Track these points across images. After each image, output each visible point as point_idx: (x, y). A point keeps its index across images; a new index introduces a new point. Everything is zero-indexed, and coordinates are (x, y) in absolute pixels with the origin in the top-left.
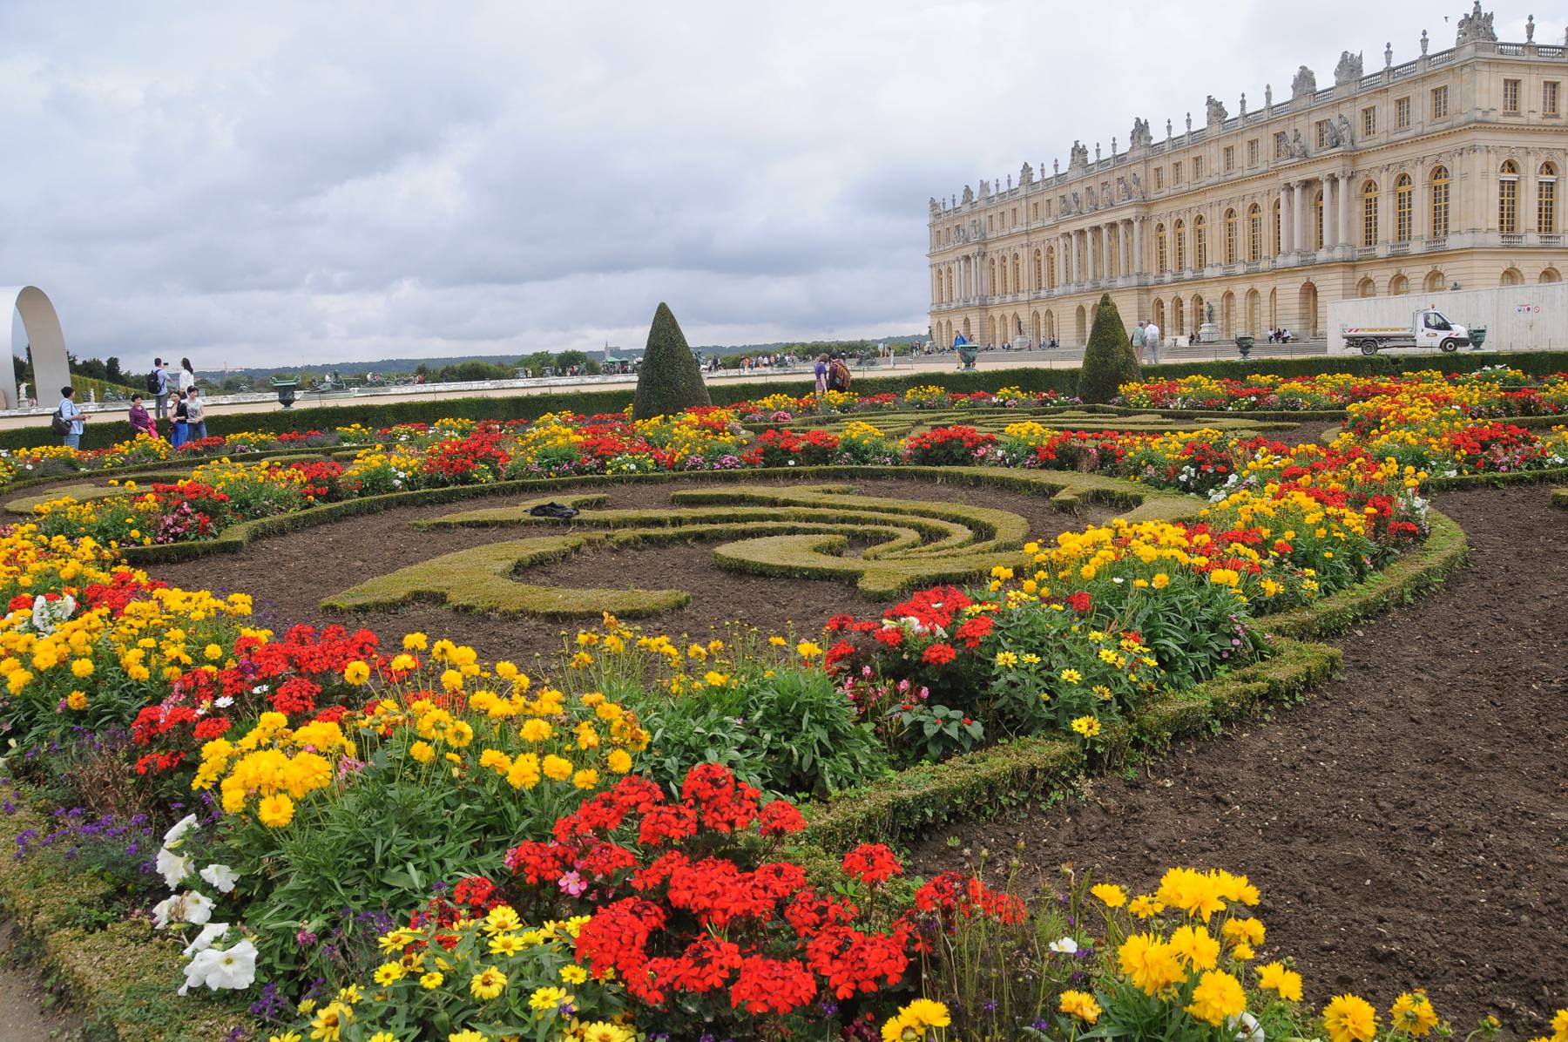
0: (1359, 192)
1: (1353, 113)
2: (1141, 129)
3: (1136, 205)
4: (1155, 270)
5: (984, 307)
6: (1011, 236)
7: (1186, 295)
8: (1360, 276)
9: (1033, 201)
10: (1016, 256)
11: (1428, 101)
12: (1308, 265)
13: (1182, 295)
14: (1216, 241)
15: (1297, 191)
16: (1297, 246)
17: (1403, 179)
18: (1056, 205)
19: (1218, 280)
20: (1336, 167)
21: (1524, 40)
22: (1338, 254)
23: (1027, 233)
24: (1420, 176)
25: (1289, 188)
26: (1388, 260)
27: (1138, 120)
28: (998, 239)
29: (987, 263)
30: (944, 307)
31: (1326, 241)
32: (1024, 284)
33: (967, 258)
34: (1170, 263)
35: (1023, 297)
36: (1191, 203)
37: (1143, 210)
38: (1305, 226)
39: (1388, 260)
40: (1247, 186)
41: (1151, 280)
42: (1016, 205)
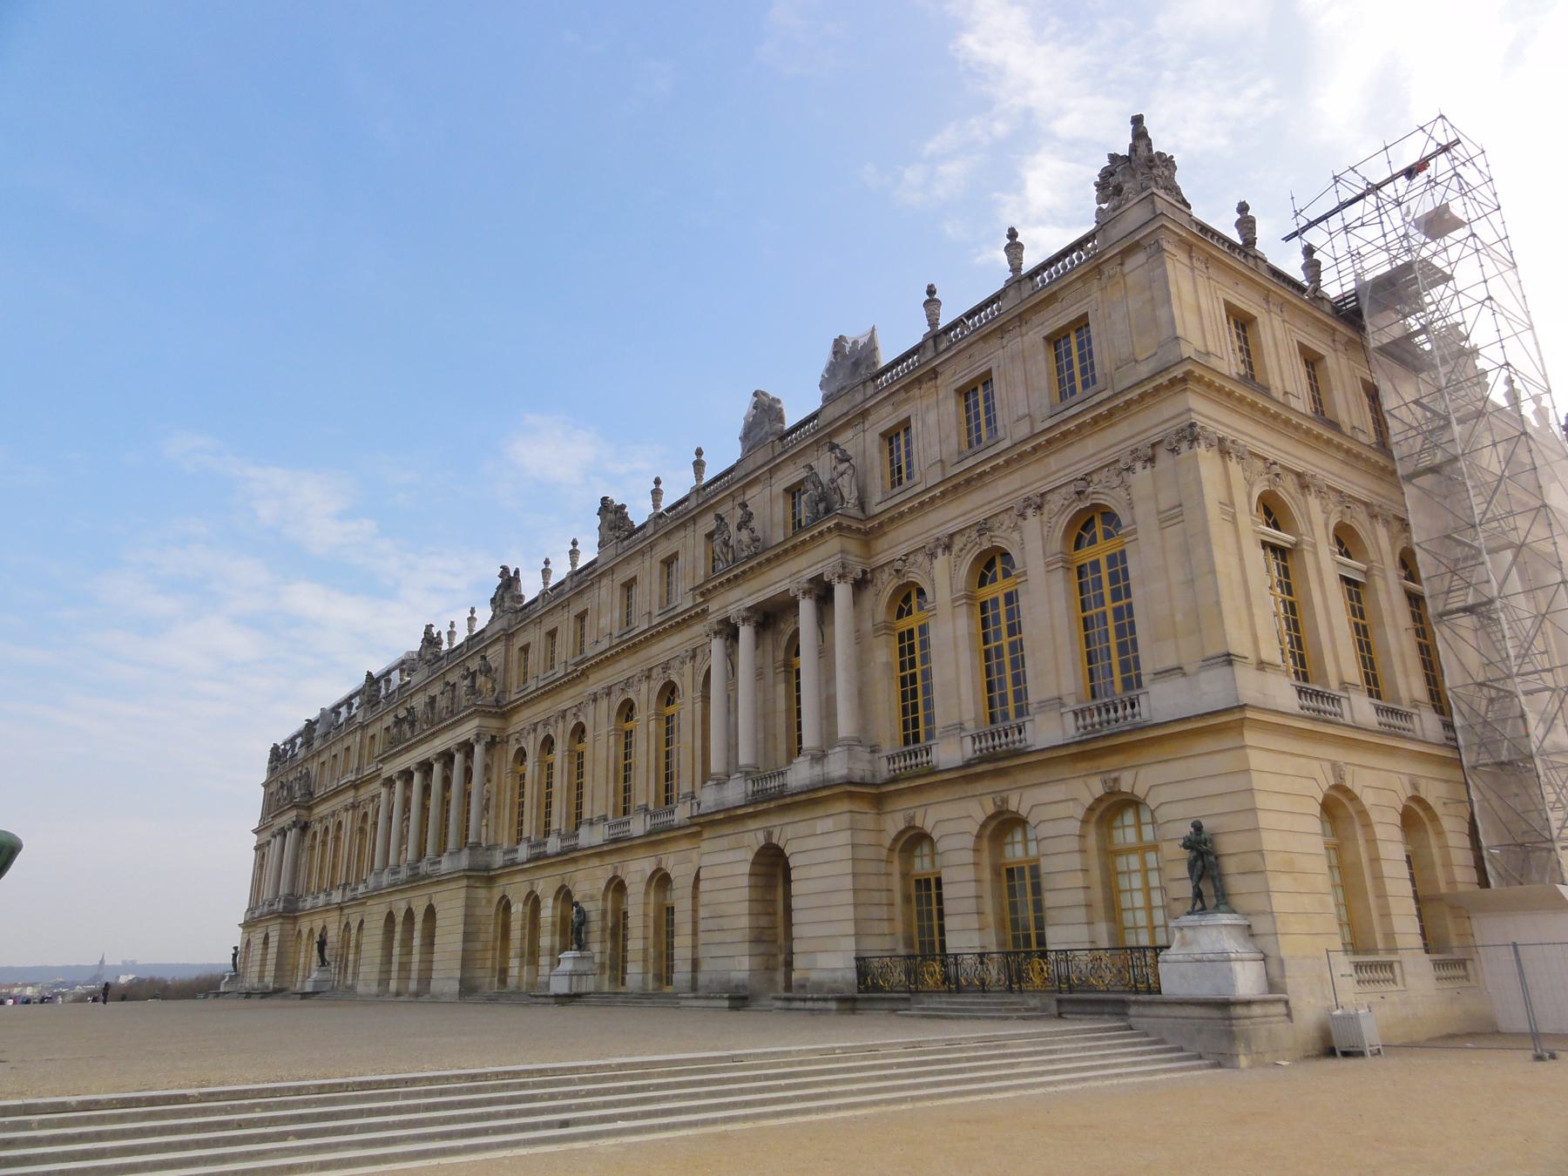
0: (881, 613)
1: (864, 443)
6: (337, 793)
7: (546, 887)
8: (894, 823)
9: (371, 732)
12: (772, 800)
14: (601, 771)
15: (746, 633)
16: (745, 758)
17: (992, 563)
19: (599, 853)
20: (822, 558)
23: (355, 786)
24: (1035, 547)
25: (729, 632)
26: (967, 774)
27: (505, 569)
31: (809, 739)
33: (283, 832)
35: (337, 897)
37: (494, 724)
38: (763, 715)
39: (967, 774)
41: (498, 859)
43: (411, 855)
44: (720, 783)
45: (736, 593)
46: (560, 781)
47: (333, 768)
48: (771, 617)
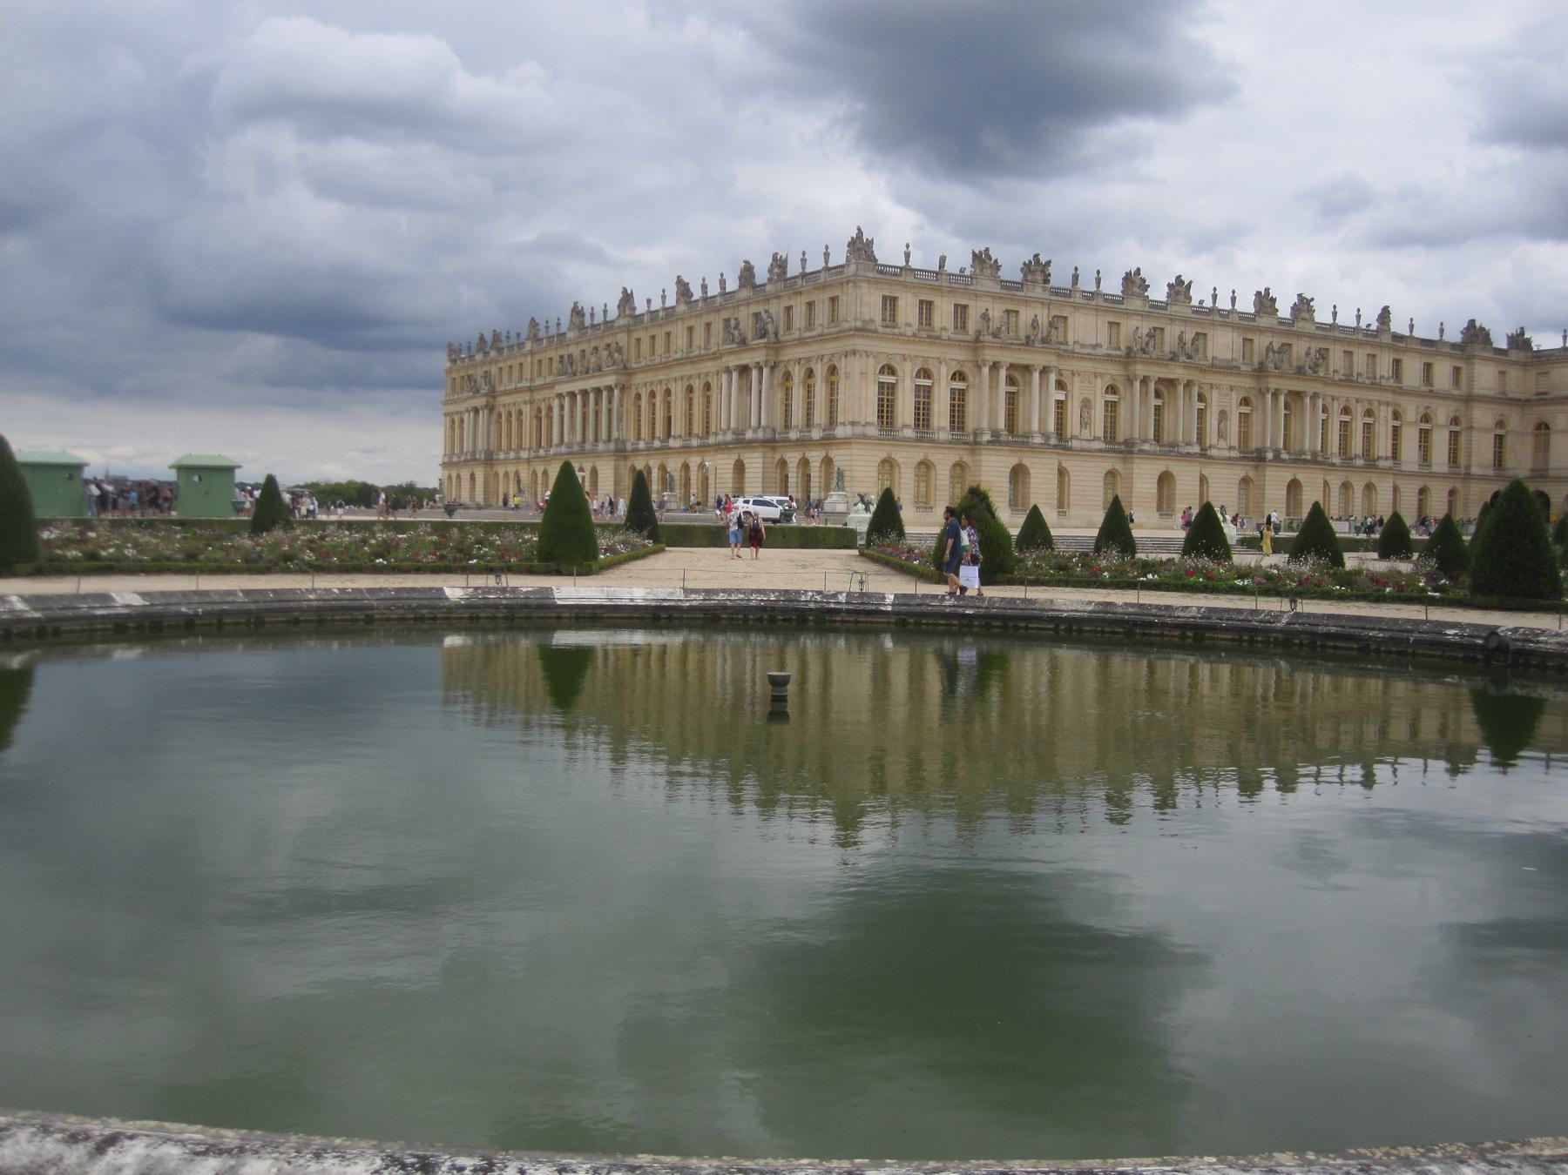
2: (627, 298)
3: (616, 372)
4: (632, 437)
5: (489, 460)
6: (516, 391)
8: (778, 456)
9: (538, 357)
10: (520, 413)
11: (827, 305)
12: (741, 443)
13: (651, 463)
15: (735, 375)
18: (556, 364)
21: (903, 264)
22: (760, 435)
23: (530, 390)
24: (820, 370)
25: (728, 371)
28: (506, 393)
29: (495, 416)
30: (455, 459)
32: (526, 442)
34: (645, 433)
35: (524, 455)
36: (661, 376)
37: (623, 379)
40: (702, 365)
41: (629, 447)
42: (522, 360)
43: (579, 438)
44: (725, 433)
45: (732, 358)
46: (660, 415)
47: (510, 374)
48: (744, 370)
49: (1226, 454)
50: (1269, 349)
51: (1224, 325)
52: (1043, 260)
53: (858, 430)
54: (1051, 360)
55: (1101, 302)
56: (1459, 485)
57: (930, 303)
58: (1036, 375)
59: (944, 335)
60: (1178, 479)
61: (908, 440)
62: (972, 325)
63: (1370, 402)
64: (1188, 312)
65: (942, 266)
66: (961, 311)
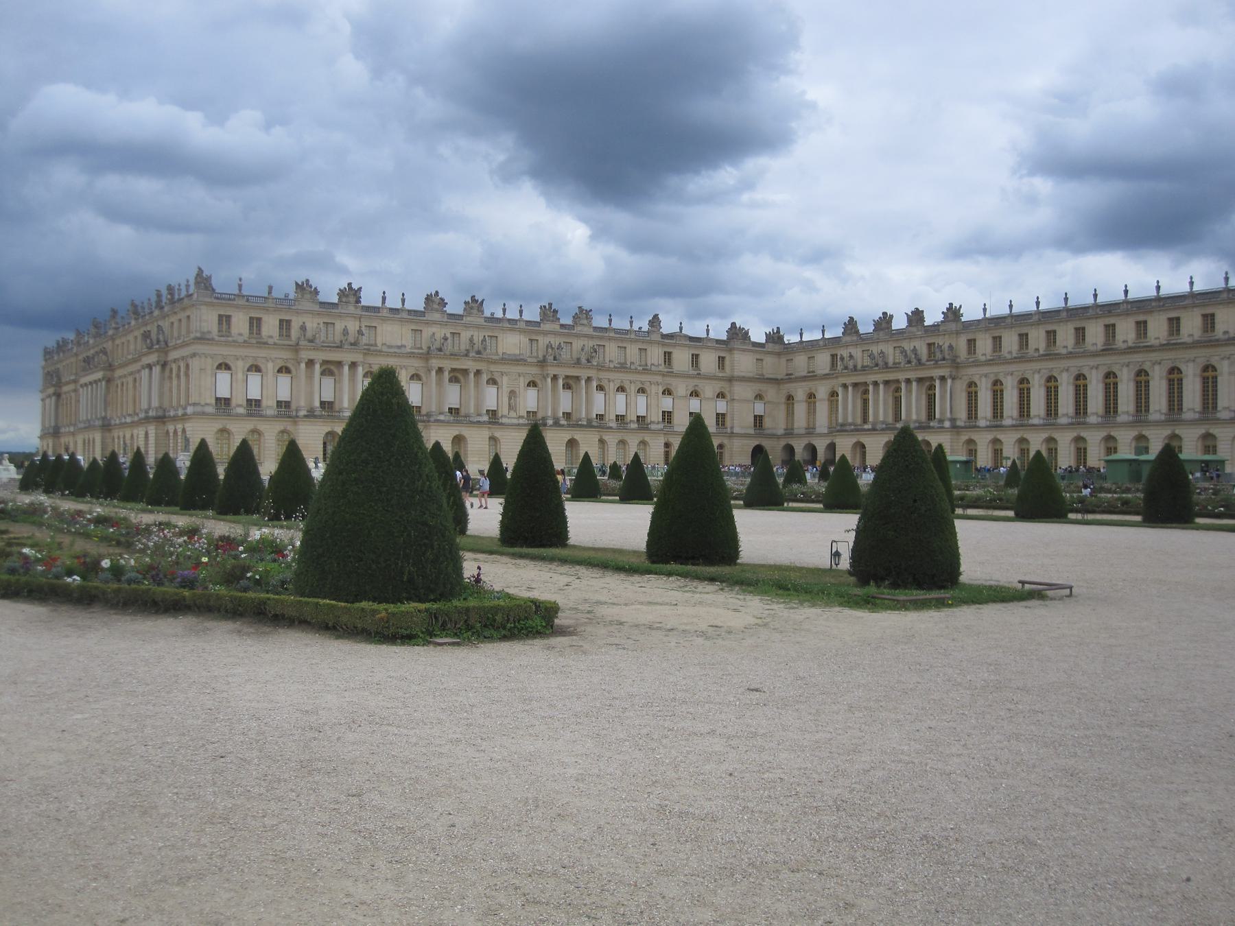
3: (103, 369)
21: (237, 292)
37: (109, 374)
49: (515, 421)
50: (549, 346)
51: (512, 330)
52: (355, 287)
53: (198, 409)
54: (358, 357)
55: (405, 315)
56: (726, 441)
57: (259, 320)
58: (346, 368)
59: (271, 341)
60: (470, 441)
61: (238, 415)
62: (295, 332)
63: (642, 383)
64: (482, 321)
65: (270, 293)
66: (285, 325)
